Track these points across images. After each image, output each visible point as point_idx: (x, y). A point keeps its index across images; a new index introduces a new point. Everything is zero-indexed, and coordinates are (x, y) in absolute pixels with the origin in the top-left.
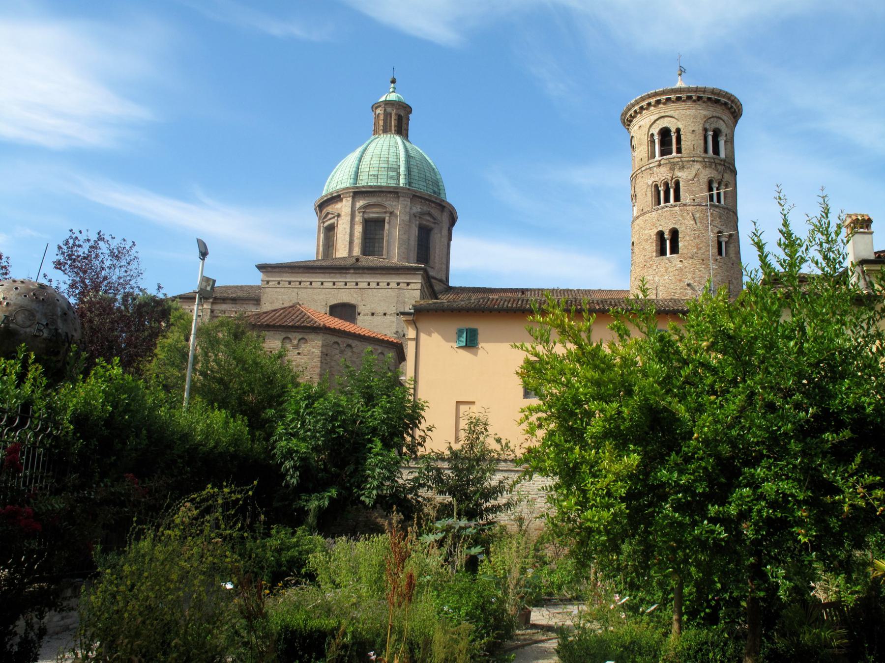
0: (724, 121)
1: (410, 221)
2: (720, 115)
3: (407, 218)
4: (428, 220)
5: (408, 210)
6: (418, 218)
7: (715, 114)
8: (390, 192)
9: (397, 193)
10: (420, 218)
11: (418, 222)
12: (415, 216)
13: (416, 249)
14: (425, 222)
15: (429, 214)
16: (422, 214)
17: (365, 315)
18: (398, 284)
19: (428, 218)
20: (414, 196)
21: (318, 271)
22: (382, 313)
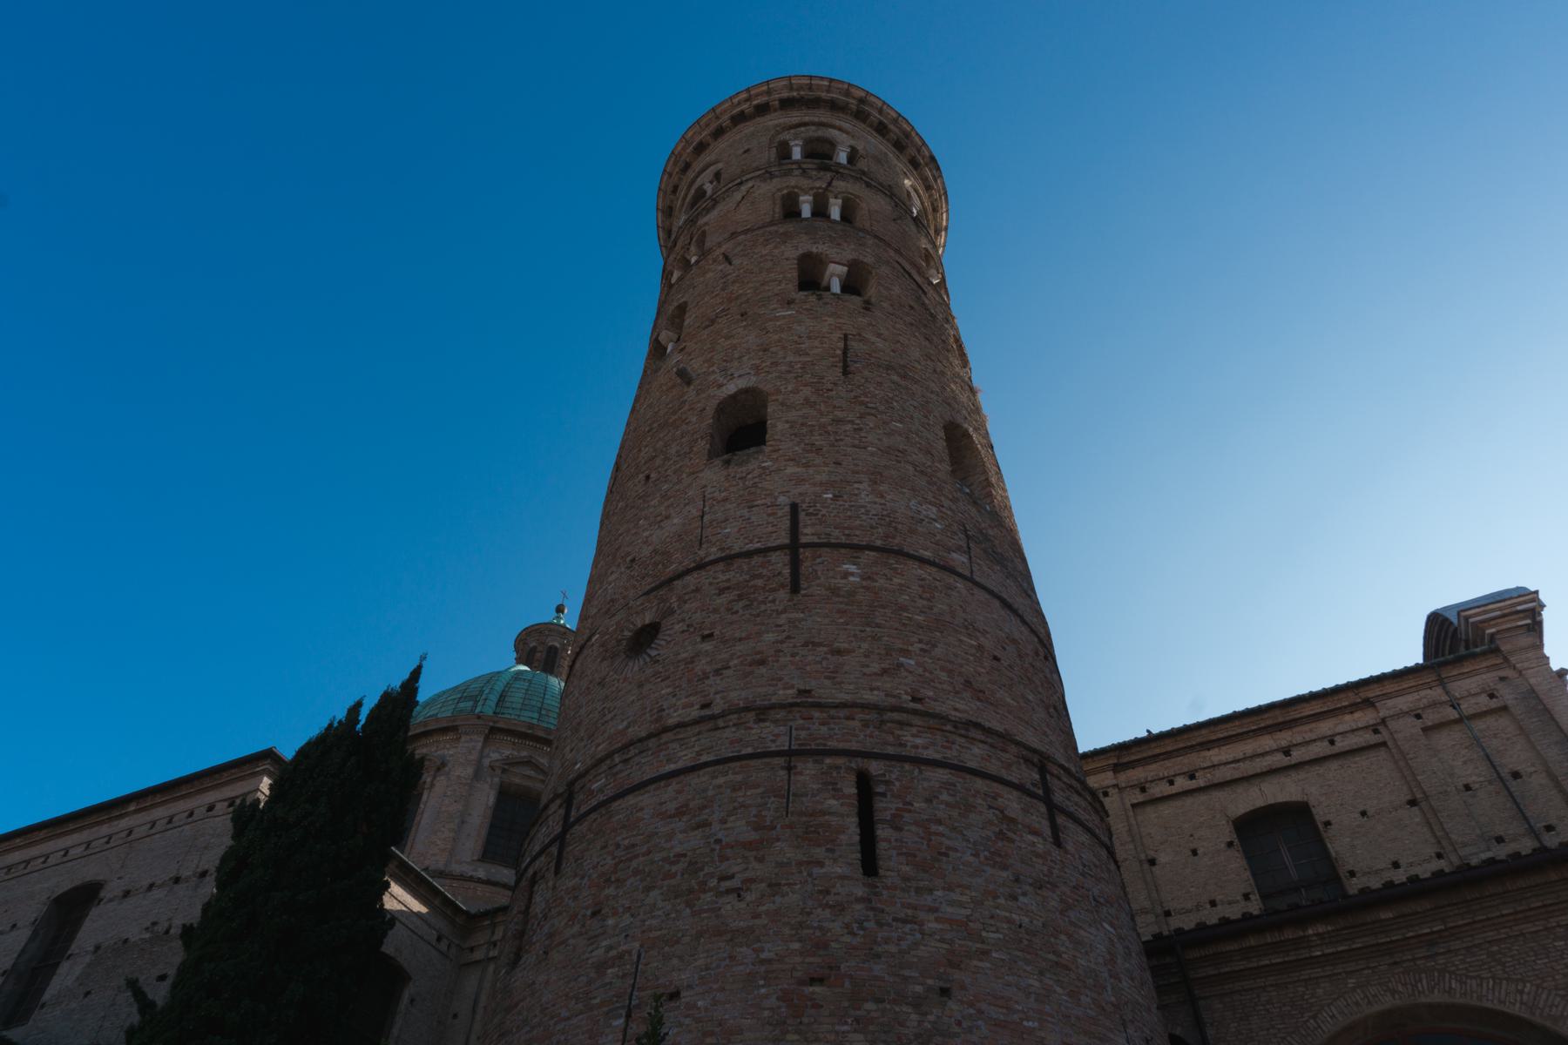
0: (840, 129)
1: (477, 775)
2: (823, 120)
3: (470, 771)
4: (529, 777)
5: (474, 757)
6: (498, 772)
7: (807, 119)
8: (444, 730)
9: (454, 729)
10: (504, 771)
11: (497, 780)
12: (492, 768)
13: (484, 833)
14: (517, 780)
15: (528, 763)
16: (509, 764)
17: (111, 900)
18: (211, 808)
19: (532, 773)
20: (494, 730)
21: (71, 826)
22: (146, 883)
